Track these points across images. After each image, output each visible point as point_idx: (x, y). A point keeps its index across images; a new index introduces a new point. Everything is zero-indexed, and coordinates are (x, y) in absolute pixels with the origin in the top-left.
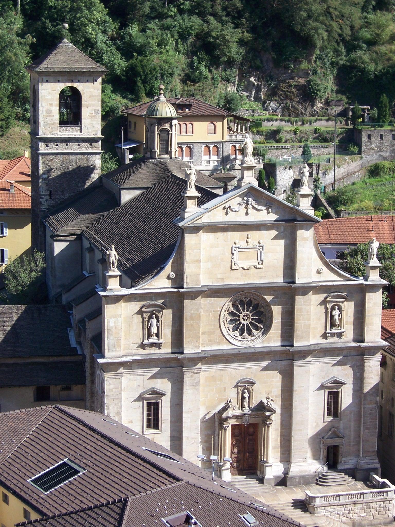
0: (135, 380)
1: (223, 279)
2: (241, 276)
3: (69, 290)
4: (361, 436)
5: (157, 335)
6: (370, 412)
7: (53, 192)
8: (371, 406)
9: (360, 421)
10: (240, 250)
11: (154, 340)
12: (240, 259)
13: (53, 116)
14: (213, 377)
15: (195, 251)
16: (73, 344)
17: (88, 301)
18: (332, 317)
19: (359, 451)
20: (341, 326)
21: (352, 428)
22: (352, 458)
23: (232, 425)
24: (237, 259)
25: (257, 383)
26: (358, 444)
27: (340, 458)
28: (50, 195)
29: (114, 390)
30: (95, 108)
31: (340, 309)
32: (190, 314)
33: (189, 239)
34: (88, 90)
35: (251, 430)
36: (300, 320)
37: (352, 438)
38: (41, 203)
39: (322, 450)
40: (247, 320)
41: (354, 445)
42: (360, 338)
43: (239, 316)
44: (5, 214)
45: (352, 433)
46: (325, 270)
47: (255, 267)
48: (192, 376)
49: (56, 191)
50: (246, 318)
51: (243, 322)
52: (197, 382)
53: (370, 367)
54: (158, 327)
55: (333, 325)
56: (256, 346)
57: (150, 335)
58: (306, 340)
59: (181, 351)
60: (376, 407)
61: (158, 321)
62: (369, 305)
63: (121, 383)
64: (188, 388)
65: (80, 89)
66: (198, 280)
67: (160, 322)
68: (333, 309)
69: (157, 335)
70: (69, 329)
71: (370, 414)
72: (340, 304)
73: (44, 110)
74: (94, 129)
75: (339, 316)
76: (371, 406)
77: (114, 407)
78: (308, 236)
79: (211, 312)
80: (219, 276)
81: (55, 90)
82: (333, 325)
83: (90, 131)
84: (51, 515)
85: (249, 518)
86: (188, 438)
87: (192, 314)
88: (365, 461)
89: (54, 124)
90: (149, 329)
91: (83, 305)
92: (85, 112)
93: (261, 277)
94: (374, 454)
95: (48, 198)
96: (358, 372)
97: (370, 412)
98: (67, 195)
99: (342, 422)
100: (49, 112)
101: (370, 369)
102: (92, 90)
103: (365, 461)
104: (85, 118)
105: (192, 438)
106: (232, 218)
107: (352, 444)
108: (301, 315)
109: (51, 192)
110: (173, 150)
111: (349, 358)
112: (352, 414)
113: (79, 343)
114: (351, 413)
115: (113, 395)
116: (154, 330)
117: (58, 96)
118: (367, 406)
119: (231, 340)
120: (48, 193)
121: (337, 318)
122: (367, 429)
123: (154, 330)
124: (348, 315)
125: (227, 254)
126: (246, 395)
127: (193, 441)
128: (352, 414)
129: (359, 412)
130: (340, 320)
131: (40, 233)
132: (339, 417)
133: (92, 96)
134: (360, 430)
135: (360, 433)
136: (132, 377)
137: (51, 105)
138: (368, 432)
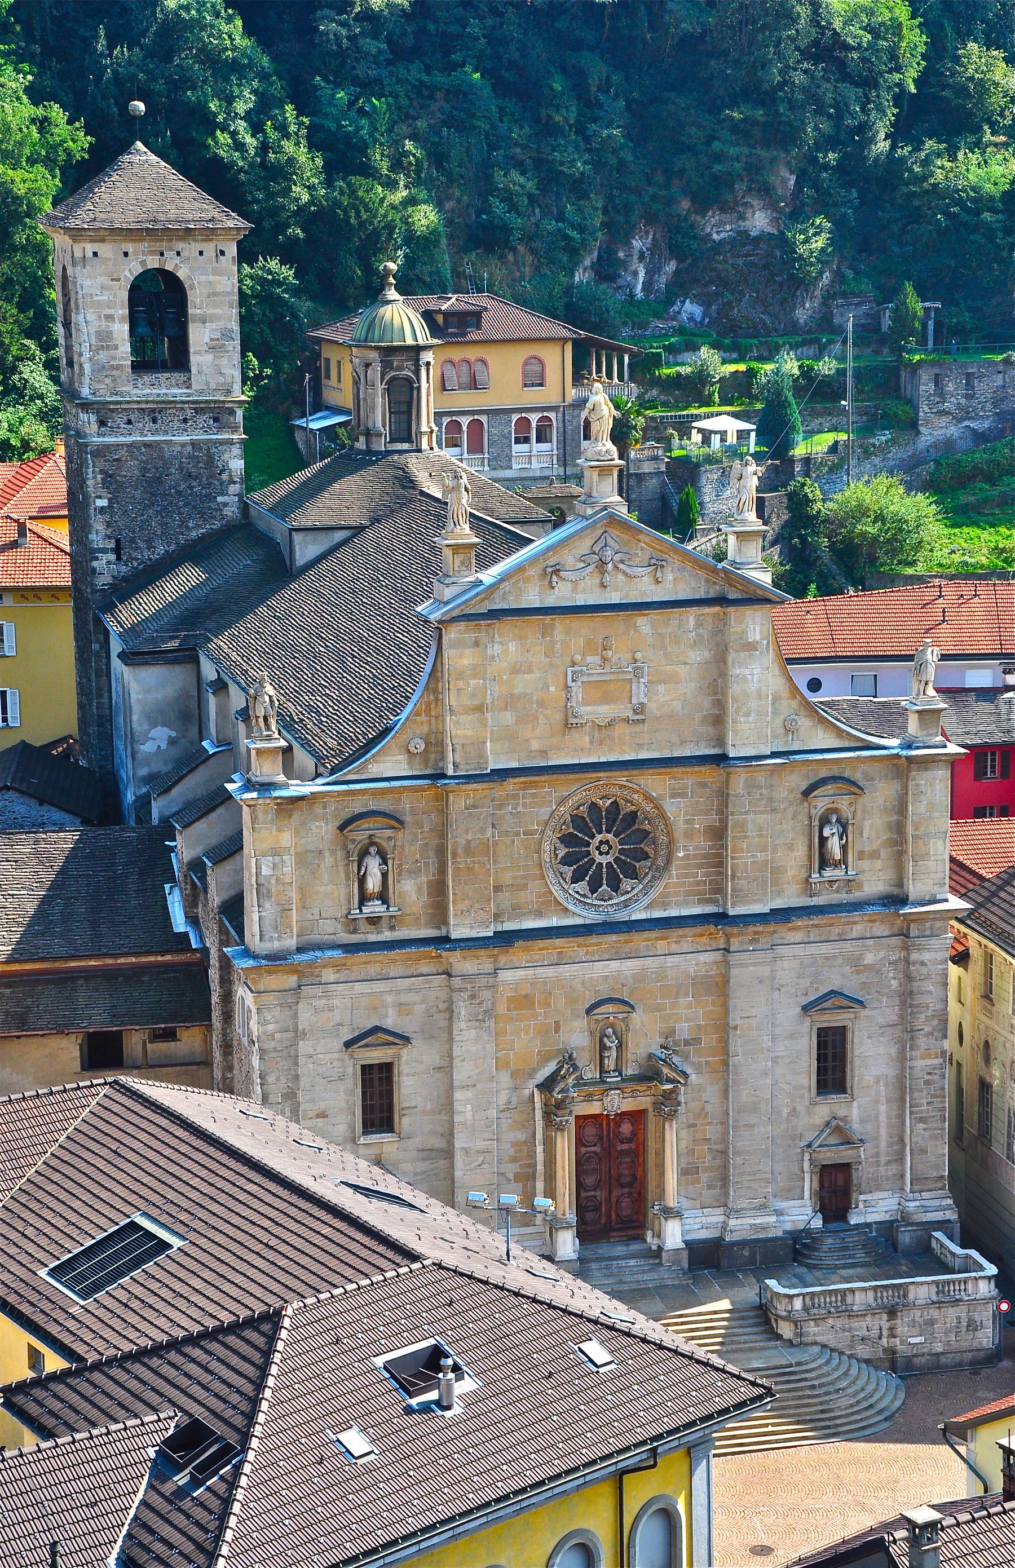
0: (331, 1009)
1: (544, 753)
2: (591, 742)
3: (168, 790)
4: (907, 1140)
5: (383, 897)
6: (927, 1077)
7: (124, 543)
8: (928, 1062)
9: (902, 1100)
11: (375, 908)
12: (585, 703)
13: (116, 347)
14: (526, 996)
15: (472, 682)
16: (179, 923)
17: (213, 816)
18: (823, 841)
19: (902, 1176)
20: (846, 864)
21: (883, 1119)
22: (885, 1194)
23: (578, 1118)
24: (577, 702)
26: (900, 1159)
27: (854, 1195)
28: (118, 550)
29: (277, 1036)
30: (222, 324)
32: (464, 842)
33: (460, 653)
34: (203, 278)
35: (626, 1128)
37: (883, 1144)
38: (94, 570)
39: (807, 1176)
40: (607, 853)
42: (896, 891)
43: (588, 844)
44: (8, 600)
45: (883, 1132)
46: (804, 723)
47: (627, 720)
49: (132, 540)
50: (605, 848)
51: (599, 859)
52: (485, 1012)
53: (923, 963)
54: (385, 875)
55: (824, 862)
56: (633, 918)
57: (364, 898)
58: (760, 901)
59: (444, 933)
60: (942, 1067)
61: (385, 862)
62: (916, 809)
63: (295, 1016)
64: (463, 1025)
65: (181, 274)
66: (482, 756)
67: (390, 862)
68: (824, 821)
69: (383, 897)
70: (167, 886)
71: (927, 1083)
73: (92, 330)
74: (222, 380)
76: (928, 1062)
77: (278, 1079)
78: (758, 638)
79: (517, 834)
80: (535, 745)
81: (118, 280)
83: (213, 386)
84: (91, 1358)
85: (596, 1350)
86: (466, 1151)
87: (468, 842)
88: (917, 1203)
89: (117, 367)
90: (362, 881)
91: (201, 826)
92: (198, 336)
93: (640, 746)
94: (940, 1185)
95: (113, 557)
96: (894, 978)
97: (927, 1077)
98: (161, 550)
99: (855, 1104)
100: (105, 340)
101: (924, 970)
102: (211, 278)
103: (917, 1203)
104: (199, 353)
105: (478, 1152)
106: (562, 595)
107: (883, 1160)
108: (746, 837)
109: (118, 542)
110: (424, 428)
111: (871, 942)
112: (882, 1083)
113: (193, 920)
114: (877, 1082)
115: (275, 1050)
116: (373, 884)
117: (125, 295)
118: (919, 1063)
119: (571, 907)
120: (112, 545)
121: (834, 845)
122: (921, 1120)
123: (373, 884)
124: (865, 835)
125: (552, 689)
126: (612, 1043)
127: (481, 1159)
128: (882, 1083)
129: (901, 1078)
130: (844, 848)
131: (95, 647)
132: (849, 1091)
133: (215, 294)
134: (903, 1123)
135: (903, 1131)
136: (323, 1002)
137: (110, 318)
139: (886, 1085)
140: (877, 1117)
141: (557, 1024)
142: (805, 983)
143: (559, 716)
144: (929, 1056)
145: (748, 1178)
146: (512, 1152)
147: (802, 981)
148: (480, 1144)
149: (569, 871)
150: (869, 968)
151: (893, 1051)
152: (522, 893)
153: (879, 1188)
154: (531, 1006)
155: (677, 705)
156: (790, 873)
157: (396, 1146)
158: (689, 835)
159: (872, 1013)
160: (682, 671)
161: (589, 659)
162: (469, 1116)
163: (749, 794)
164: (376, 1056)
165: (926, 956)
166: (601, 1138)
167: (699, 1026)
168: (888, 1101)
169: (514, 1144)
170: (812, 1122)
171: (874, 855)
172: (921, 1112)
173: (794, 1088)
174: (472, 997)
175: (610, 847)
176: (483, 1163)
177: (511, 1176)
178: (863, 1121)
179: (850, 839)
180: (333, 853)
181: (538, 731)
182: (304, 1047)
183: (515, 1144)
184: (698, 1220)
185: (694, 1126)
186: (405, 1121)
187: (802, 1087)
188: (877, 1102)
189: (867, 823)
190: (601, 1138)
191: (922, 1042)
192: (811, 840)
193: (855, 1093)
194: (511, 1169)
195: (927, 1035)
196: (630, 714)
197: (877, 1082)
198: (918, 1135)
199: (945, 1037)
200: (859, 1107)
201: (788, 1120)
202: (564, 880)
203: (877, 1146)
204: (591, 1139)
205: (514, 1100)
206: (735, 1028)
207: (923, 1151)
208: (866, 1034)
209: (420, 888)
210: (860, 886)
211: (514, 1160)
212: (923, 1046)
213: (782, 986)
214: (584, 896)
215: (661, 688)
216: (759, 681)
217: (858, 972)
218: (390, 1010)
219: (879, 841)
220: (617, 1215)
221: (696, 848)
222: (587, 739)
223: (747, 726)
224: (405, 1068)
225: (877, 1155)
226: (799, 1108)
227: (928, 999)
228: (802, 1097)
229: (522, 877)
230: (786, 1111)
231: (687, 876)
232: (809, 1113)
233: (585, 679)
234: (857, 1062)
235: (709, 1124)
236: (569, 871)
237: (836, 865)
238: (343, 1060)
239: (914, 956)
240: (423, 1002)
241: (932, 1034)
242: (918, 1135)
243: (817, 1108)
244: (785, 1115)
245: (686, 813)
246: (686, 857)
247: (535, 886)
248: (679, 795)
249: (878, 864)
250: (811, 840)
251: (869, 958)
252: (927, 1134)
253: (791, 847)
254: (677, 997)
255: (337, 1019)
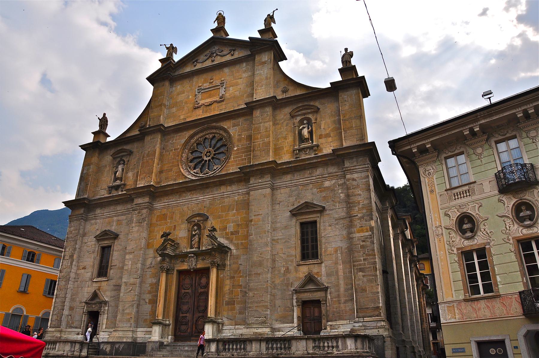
2: (202, 112)
8: (362, 234)
10: (203, 91)
11: (118, 182)
14: (164, 214)
20: (312, 139)
21: (341, 273)
23: (177, 270)
25: (210, 218)
29: (73, 232)
31: (309, 123)
36: (258, 139)
37: (342, 289)
40: (209, 156)
41: (346, 302)
45: (342, 282)
48: (139, 213)
50: (209, 154)
52: (143, 219)
53: (354, 180)
60: (371, 237)
64: (134, 225)
68: (301, 122)
69: (121, 179)
71: (362, 247)
72: (310, 116)
75: (308, 128)
76: (362, 234)
78: (266, 59)
80: (182, 117)
82: (302, 139)
87: (149, 152)
88: (361, 324)
96: (342, 193)
99: (323, 265)
101: (354, 183)
103: (361, 324)
105: (131, 284)
107: (343, 299)
108: (259, 133)
114: (336, 251)
121: (305, 132)
122: (361, 270)
125: (190, 97)
128: (339, 252)
130: (311, 133)
138: (363, 276)
139: (342, 253)
140: (337, 272)
141: (175, 226)
142: (292, 199)
143: (191, 106)
144: (362, 231)
145: (256, 305)
146: (149, 288)
147: (291, 199)
148: (132, 280)
149: (192, 164)
150: (327, 188)
151: (345, 232)
152: (170, 173)
153: (341, 319)
154: (165, 219)
155: (237, 93)
156: (285, 149)
157: (106, 283)
158: (239, 140)
159: (330, 212)
160: (240, 81)
161: (205, 85)
162: (130, 267)
163: (262, 116)
164: (106, 243)
165: (355, 176)
166: (192, 286)
167: (238, 225)
168: (343, 263)
169: (151, 285)
170: (298, 275)
171: (328, 136)
172: (360, 265)
173: (288, 256)
174: (139, 213)
175: (210, 152)
176: (132, 290)
177: (147, 301)
178: (329, 275)
179: (314, 129)
180: (110, 166)
181: (183, 113)
182: (86, 239)
183: (151, 285)
184: (231, 331)
185: (233, 277)
186: (112, 271)
187: (291, 256)
188: (336, 263)
189: (323, 123)
190: (192, 286)
191: (357, 223)
192: (295, 134)
193: (323, 257)
194: (148, 297)
195: (360, 218)
196: (218, 99)
197: (336, 251)
198: (359, 280)
199: (372, 219)
200: (326, 266)
201: (284, 274)
202: (190, 168)
203: (338, 291)
204: (187, 286)
205: (153, 263)
206: (251, 221)
207: (364, 290)
208: (327, 224)
209: (134, 175)
210: (321, 150)
211: (150, 292)
212: (358, 225)
213: (281, 202)
214: (197, 173)
215: (231, 88)
216: (267, 74)
217: (321, 192)
218: (115, 223)
219: (330, 129)
220: (196, 328)
221: (242, 145)
222: (201, 111)
223: (261, 90)
224: (115, 248)
225: (339, 296)
226: (290, 268)
227: (360, 198)
228: (292, 261)
229: (171, 166)
230: (283, 270)
231: (237, 157)
232: (296, 271)
233: (203, 91)
234: (323, 241)
235: (241, 277)
236: (192, 164)
237: (307, 140)
238: (95, 245)
239: (348, 176)
240: (126, 219)
241: (362, 217)
242: (359, 280)
243: (301, 267)
244: (282, 272)
245: (239, 132)
246: (238, 150)
247: (175, 169)
248: (236, 126)
249: (330, 139)
250: (295, 134)
251: (327, 184)
252: (365, 279)
253: (285, 138)
254: (228, 210)
255: (97, 228)
